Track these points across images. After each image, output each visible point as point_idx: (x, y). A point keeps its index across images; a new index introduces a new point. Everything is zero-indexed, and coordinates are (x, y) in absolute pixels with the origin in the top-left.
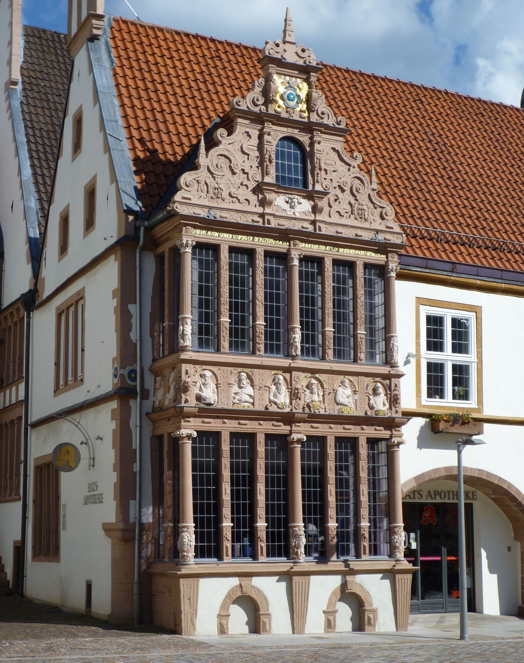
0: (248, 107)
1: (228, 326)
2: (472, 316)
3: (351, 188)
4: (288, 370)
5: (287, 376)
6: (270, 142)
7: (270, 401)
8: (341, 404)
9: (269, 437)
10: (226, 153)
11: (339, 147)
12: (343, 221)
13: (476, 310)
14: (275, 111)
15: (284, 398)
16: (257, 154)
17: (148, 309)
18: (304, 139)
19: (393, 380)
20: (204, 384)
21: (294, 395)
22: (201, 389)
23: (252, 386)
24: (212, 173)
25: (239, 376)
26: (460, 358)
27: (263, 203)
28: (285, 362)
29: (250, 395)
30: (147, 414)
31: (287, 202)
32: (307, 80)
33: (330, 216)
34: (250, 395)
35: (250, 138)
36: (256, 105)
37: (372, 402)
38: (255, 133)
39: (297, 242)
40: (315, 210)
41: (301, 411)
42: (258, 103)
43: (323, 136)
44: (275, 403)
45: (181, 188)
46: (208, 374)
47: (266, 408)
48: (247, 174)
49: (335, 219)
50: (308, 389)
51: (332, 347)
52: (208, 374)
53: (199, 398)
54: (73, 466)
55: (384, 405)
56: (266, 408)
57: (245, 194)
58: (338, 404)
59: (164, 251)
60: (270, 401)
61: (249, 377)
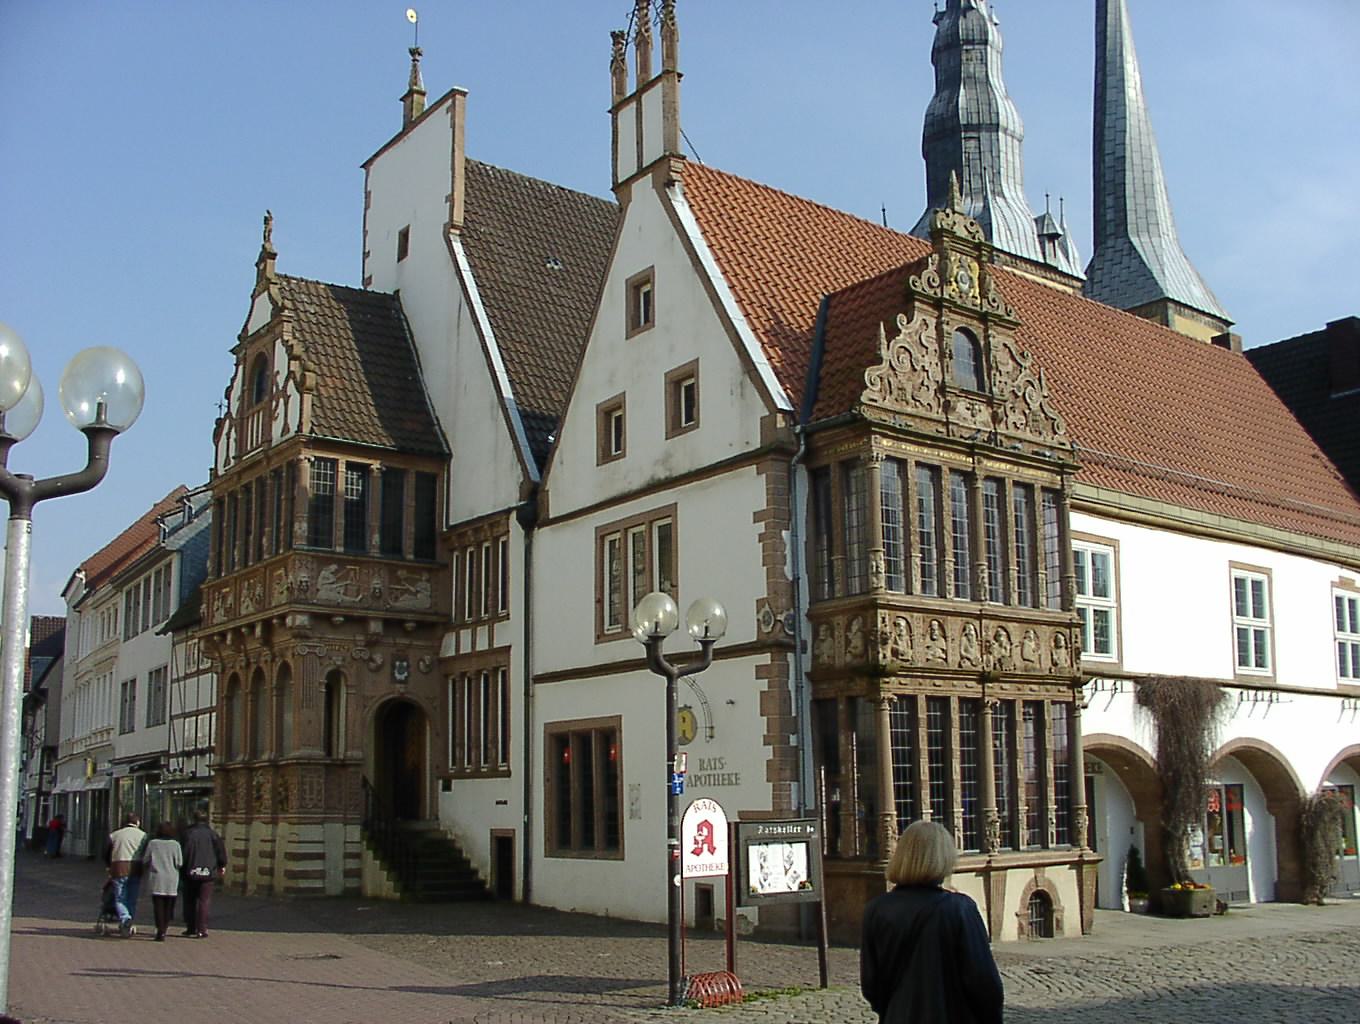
0: (923, 289)
1: (919, 563)
2: (1109, 550)
3: (1024, 394)
4: (980, 617)
5: (977, 623)
6: (949, 334)
7: (962, 657)
8: (1028, 660)
9: (962, 700)
10: (907, 346)
11: (1010, 342)
12: (1019, 434)
13: (1113, 543)
14: (950, 295)
15: (975, 652)
16: (936, 346)
17: (802, 538)
18: (977, 328)
19: (1073, 629)
20: (899, 635)
21: (986, 648)
22: (896, 643)
23: (945, 638)
24: (894, 369)
25: (931, 626)
26: (1100, 603)
27: (947, 407)
28: (975, 608)
29: (943, 650)
30: (806, 674)
31: (968, 409)
32: (978, 259)
33: (1007, 428)
34: (943, 650)
35: (927, 327)
36: (931, 287)
37: (1055, 657)
38: (932, 322)
39: (982, 459)
40: (996, 419)
41: (1047, 672)
42: (934, 284)
43: (999, 329)
44: (969, 659)
45: (867, 387)
46: (903, 623)
47: (960, 666)
48: (927, 371)
49: (1012, 432)
50: (997, 641)
51: (953, 583)
52: (903, 623)
53: (895, 653)
54: (690, 738)
55: (1066, 661)
56: (960, 666)
57: (928, 396)
58: (1024, 660)
59: (827, 467)
60: (962, 657)
61: (941, 626)
